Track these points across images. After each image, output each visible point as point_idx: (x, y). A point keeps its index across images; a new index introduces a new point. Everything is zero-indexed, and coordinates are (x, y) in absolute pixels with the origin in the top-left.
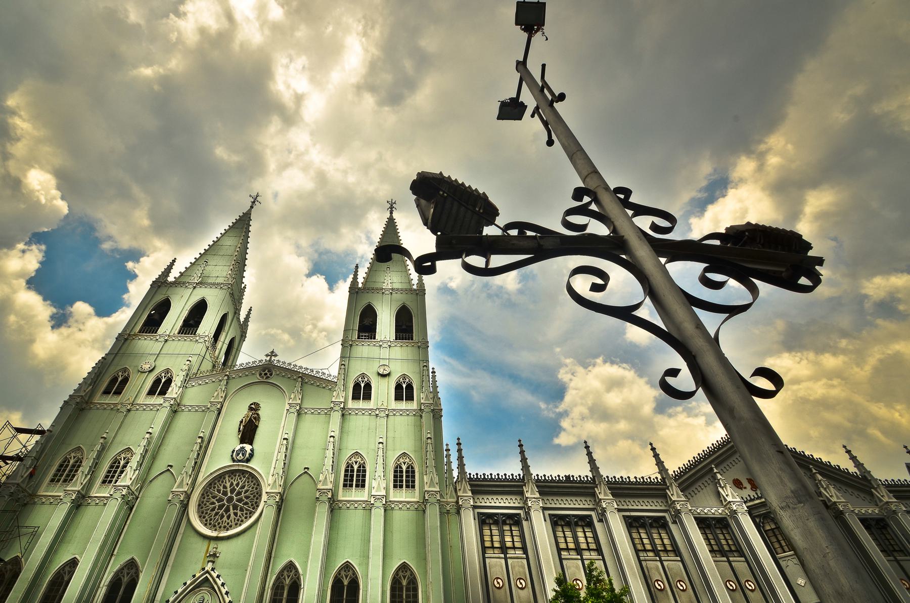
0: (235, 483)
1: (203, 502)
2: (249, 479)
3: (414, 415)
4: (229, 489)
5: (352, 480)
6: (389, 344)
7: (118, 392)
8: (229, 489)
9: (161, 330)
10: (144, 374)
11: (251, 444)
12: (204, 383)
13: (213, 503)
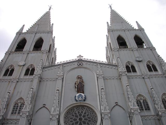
0: (80, 112)
1: (66, 121)
2: (87, 109)
3: (162, 77)
4: (78, 115)
5: (142, 107)
6: (136, 49)
7: (11, 74)
8: (78, 115)
9: (24, 50)
11: (83, 93)
13: (71, 121)
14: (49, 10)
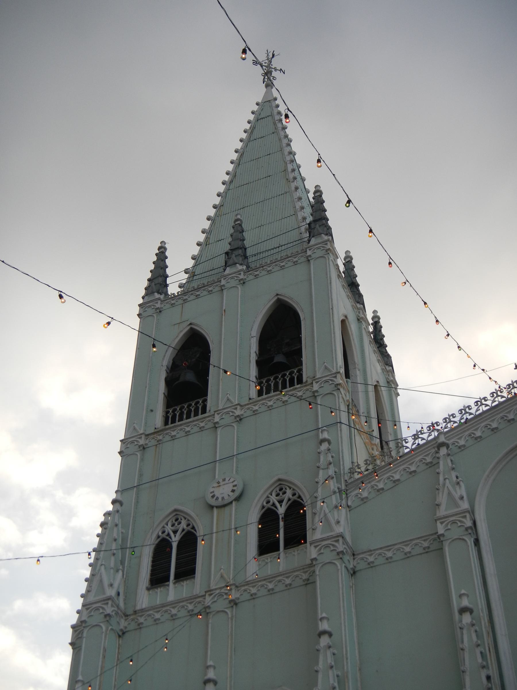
10: (227, 509)
12: (390, 484)
14: (264, 90)
